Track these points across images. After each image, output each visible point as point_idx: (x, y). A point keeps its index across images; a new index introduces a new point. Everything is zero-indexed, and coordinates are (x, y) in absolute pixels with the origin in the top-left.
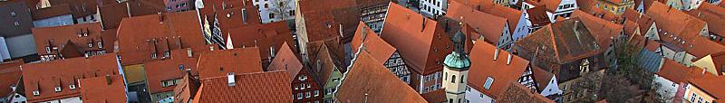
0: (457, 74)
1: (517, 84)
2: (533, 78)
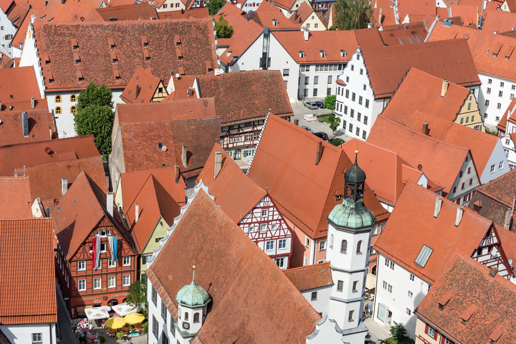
0: (352, 239)
1: (469, 261)
2: (501, 250)
